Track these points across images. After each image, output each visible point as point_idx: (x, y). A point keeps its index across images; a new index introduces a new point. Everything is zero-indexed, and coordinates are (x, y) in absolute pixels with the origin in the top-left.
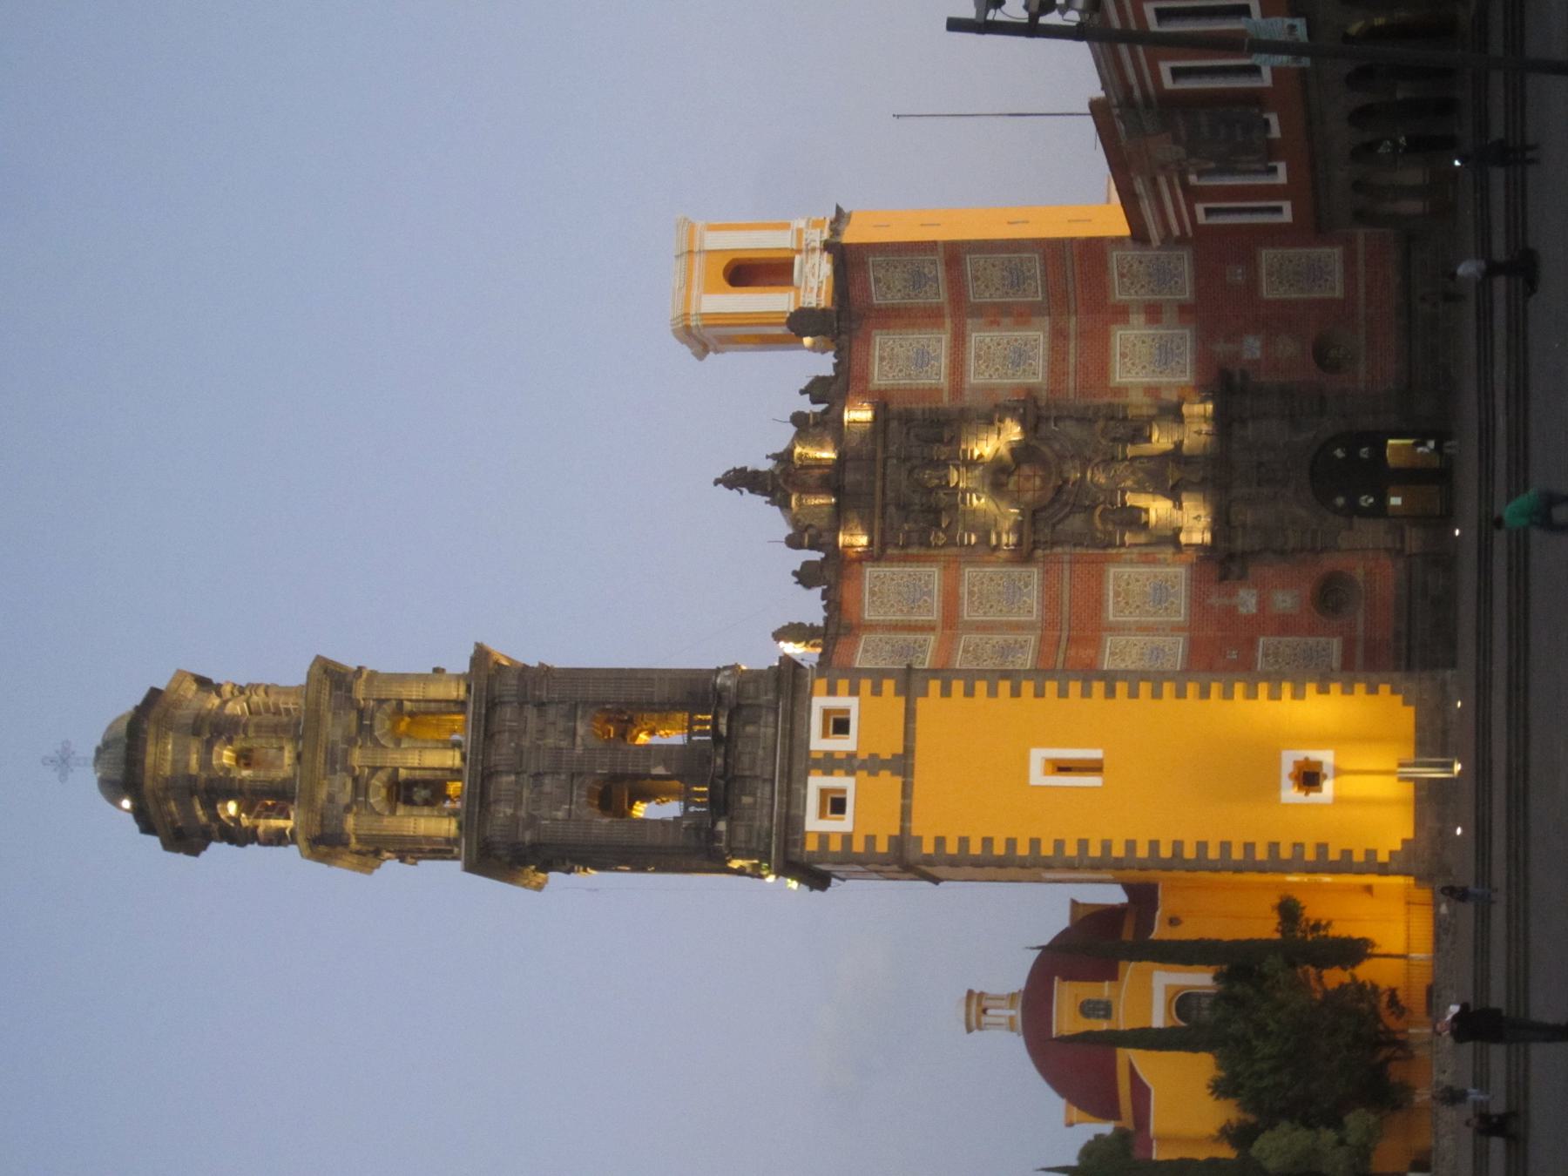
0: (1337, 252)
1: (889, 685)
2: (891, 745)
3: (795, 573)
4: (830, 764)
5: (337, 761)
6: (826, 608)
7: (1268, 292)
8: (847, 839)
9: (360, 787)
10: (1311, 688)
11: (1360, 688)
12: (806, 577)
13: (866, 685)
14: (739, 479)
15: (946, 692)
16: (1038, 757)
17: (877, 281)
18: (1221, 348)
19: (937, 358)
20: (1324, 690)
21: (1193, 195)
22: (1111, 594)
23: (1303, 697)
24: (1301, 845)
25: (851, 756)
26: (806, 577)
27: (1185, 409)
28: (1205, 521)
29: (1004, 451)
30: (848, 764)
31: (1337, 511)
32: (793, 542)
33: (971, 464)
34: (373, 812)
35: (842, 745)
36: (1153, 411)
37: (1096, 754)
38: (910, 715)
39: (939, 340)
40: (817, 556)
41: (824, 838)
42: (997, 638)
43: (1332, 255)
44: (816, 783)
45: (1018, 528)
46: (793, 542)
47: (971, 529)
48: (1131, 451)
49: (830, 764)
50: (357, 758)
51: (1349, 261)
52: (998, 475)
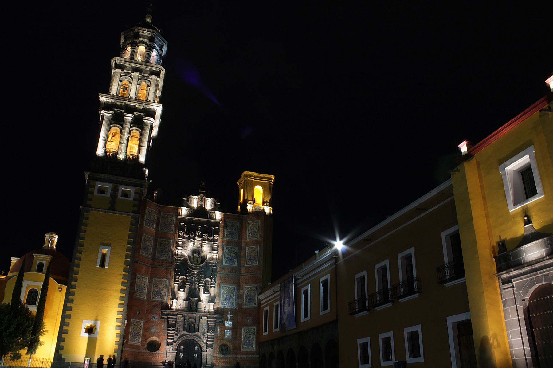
0: (254, 349)
4: (115, 190)
5: (135, 70)
7: (244, 329)
8: (92, 193)
9: (127, 74)
10: (119, 331)
11: (117, 347)
13: (137, 203)
17: (254, 222)
18: (229, 315)
20: (118, 335)
21: (271, 306)
23: (116, 329)
24: (68, 325)
25: (116, 197)
27: (212, 304)
28: (179, 307)
29: (205, 253)
31: (179, 346)
33: (201, 244)
34: (121, 76)
36: (212, 295)
41: (94, 187)
42: (151, 247)
43: (253, 348)
45: (182, 255)
47: (183, 243)
48: (201, 288)
49: (115, 190)
50: (136, 74)
51: (251, 353)
52: (197, 251)
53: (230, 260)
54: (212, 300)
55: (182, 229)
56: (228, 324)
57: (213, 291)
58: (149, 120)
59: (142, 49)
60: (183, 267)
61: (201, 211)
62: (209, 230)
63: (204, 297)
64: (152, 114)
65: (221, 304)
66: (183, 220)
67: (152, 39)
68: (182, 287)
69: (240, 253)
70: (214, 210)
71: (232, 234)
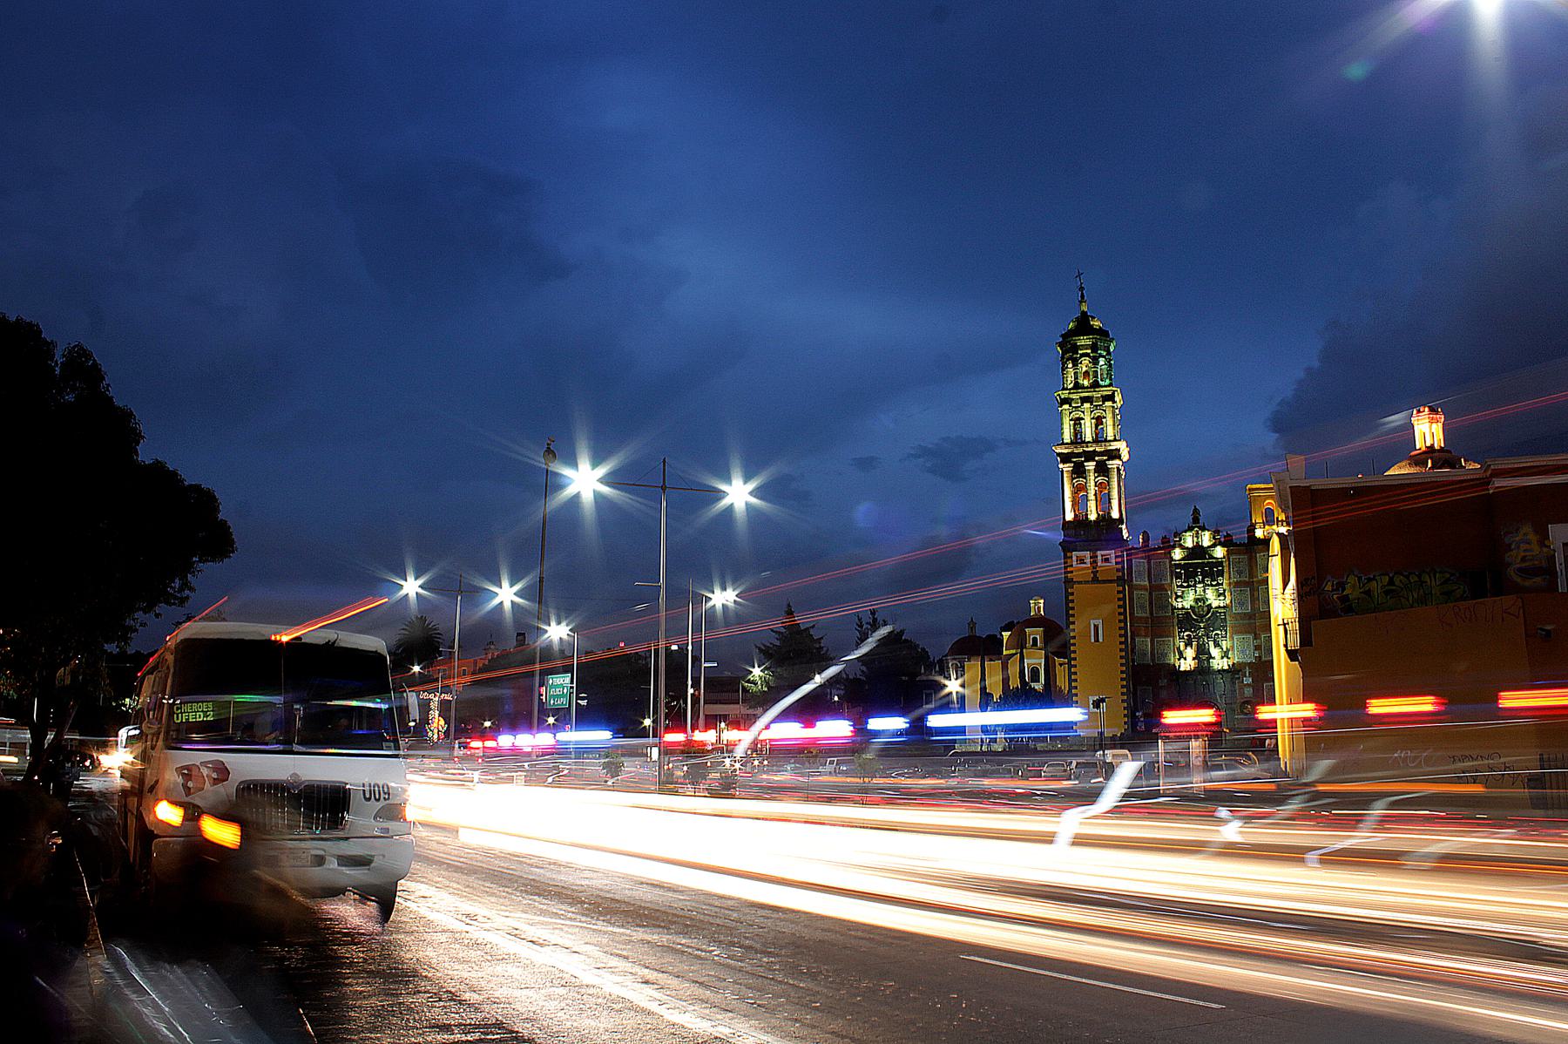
4: (1094, 557)
30: (1094, 563)
38: (1111, 581)
49: (1094, 557)
50: (1087, 405)
53: (1241, 604)
54: (1225, 655)
55: (1178, 576)
56: (1248, 680)
57: (1224, 645)
58: (1114, 464)
59: (1085, 363)
60: (1188, 621)
61: (1198, 551)
62: (1212, 571)
63: (1215, 652)
64: (1115, 454)
65: (1235, 658)
66: (1178, 566)
67: (1094, 348)
68: (1188, 644)
69: (1252, 595)
70: (1214, 546)
71: (1240, 573)
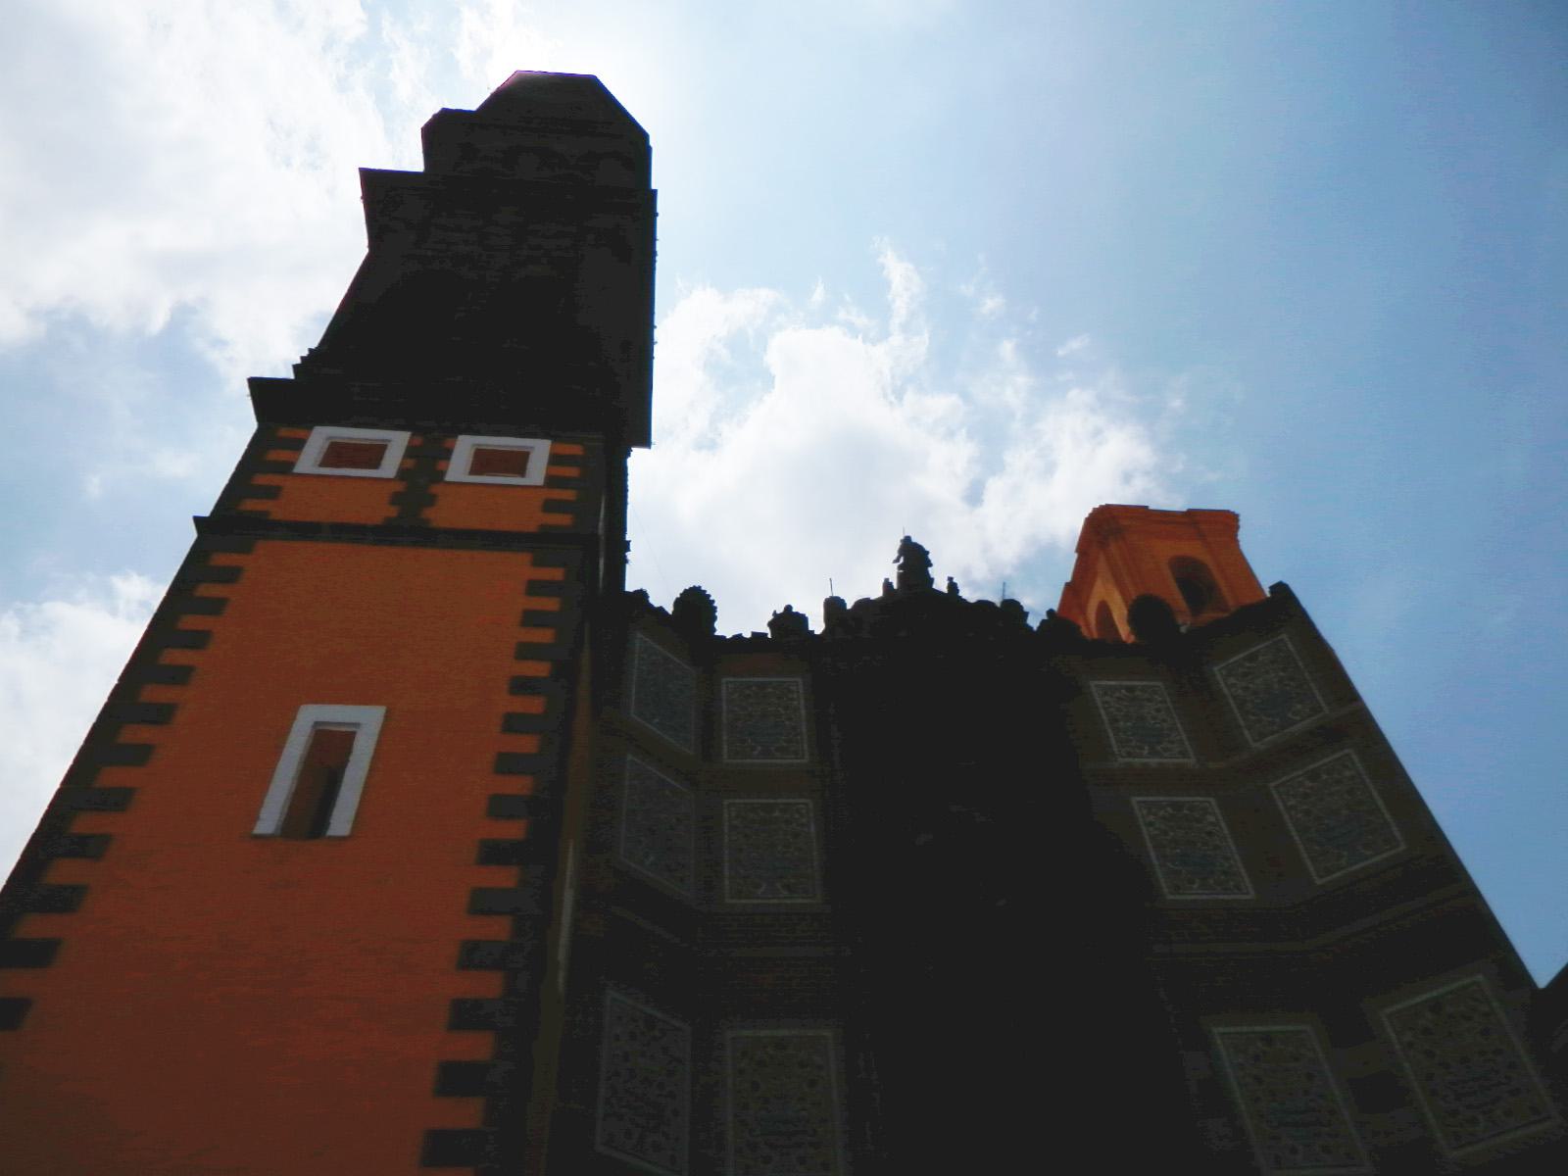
1: (562, 520)
2: (442, 515)
3: (788, 608)
6: (738, 638)
8: (286, 468)
12: (788, 622)
14: (914, 557)
15: (534, 588)
16: (367, 721)
17: (1252, 658)
19: (1153, 753)
22: (782, 1033)
26: (788, 622)
32: (833, 606)
35: (459, 466)
37: (341, 822)
39: (1184, 754)
40: (817, 625)
41: (298, 445)
44: (397, 443)
46: (833, 606)
